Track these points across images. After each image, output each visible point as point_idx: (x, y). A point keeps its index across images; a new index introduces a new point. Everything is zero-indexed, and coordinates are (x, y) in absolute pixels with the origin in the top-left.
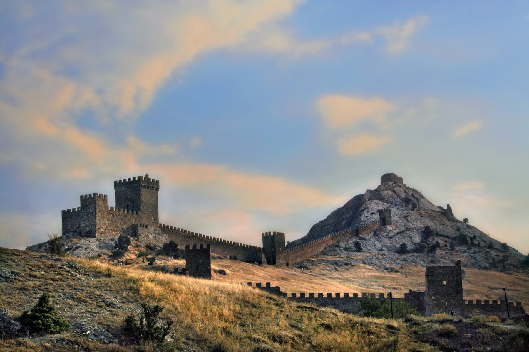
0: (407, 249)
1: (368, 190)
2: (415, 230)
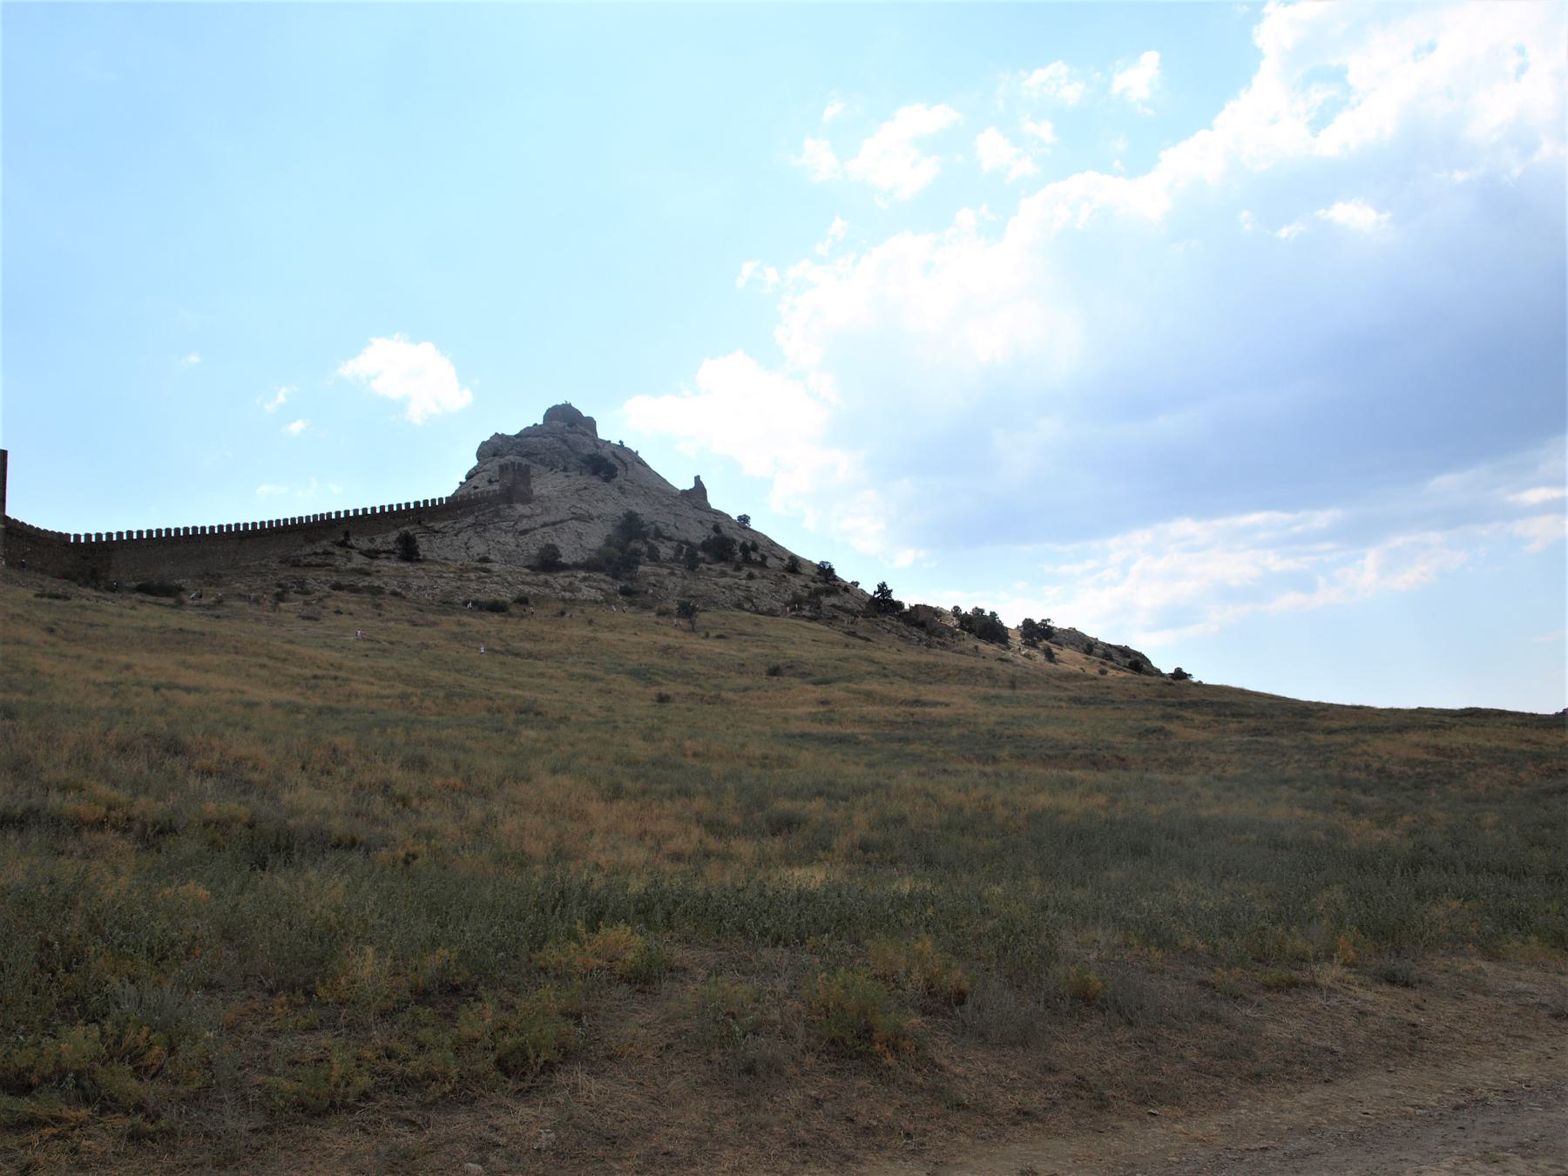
0: (560, 559)
1: (496, 434)
2: (596, 520)
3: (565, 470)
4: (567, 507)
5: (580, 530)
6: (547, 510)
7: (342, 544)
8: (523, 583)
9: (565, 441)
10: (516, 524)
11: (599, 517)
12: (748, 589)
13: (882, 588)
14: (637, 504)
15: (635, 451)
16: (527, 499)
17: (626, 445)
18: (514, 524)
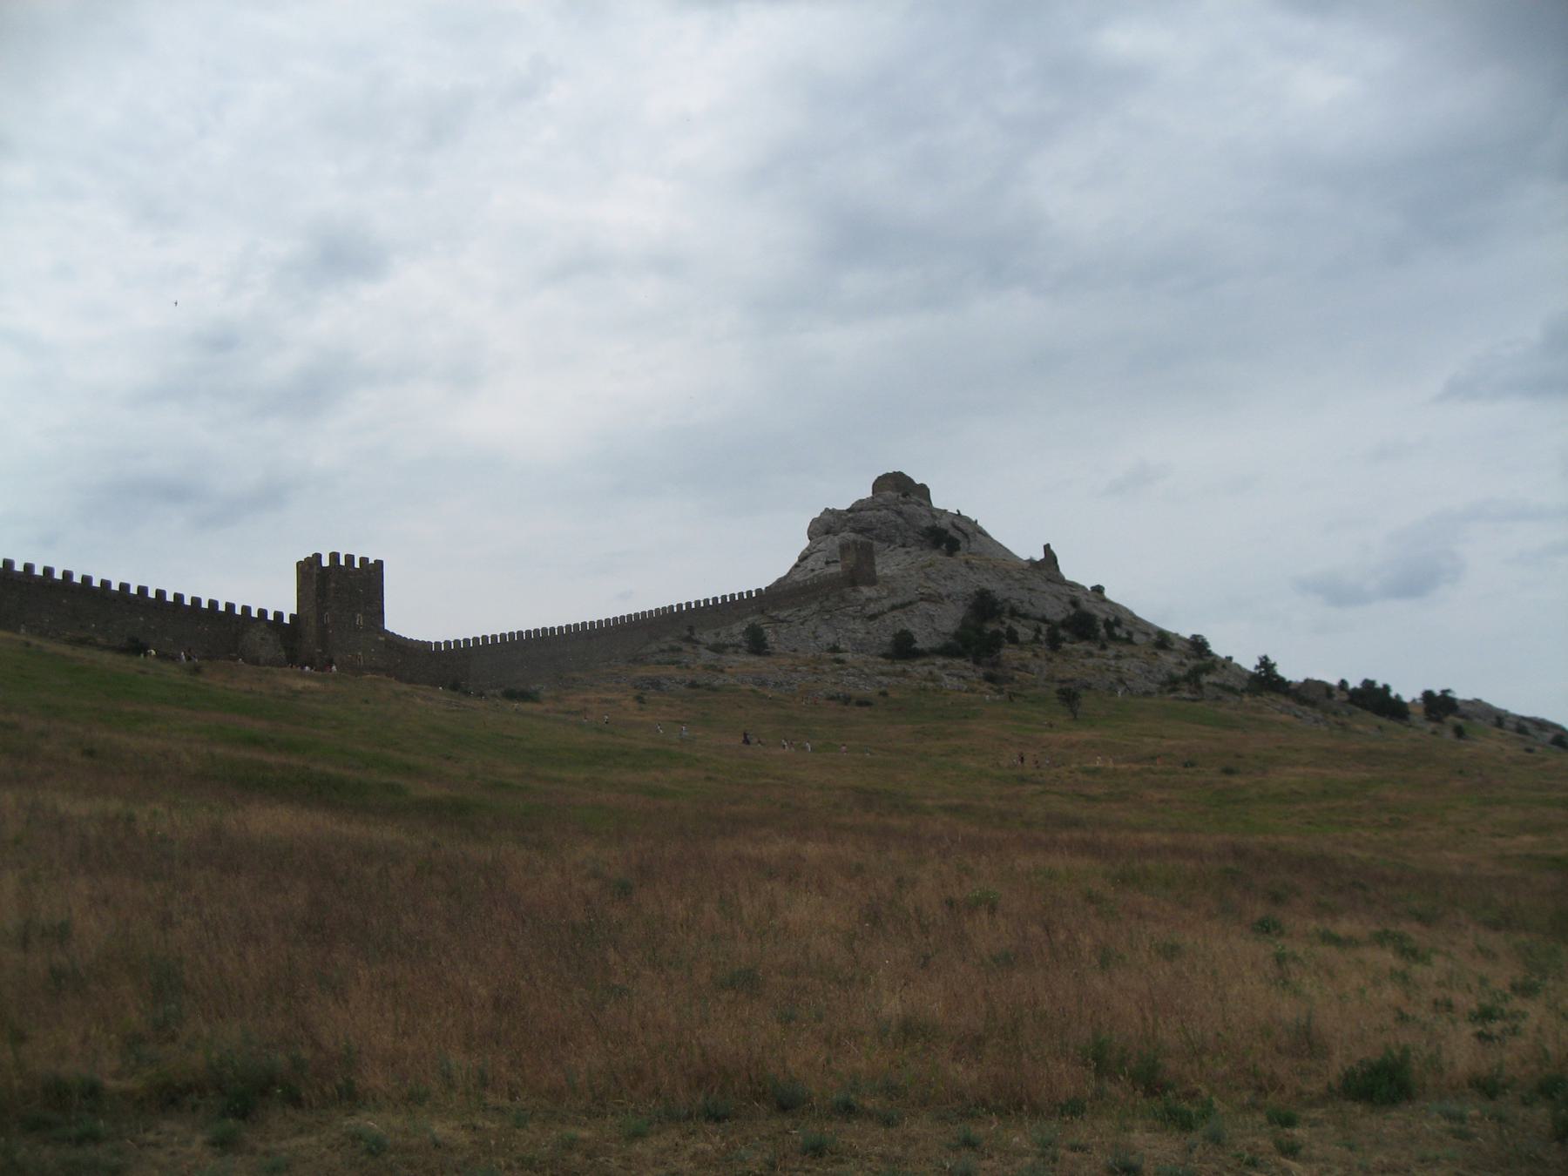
1: (827, 509)
2: (946, 599)
3: (904, 546)
4: (915, 586)
5: (931, 613)
6: (893, 592)
7: (688, 639)
8: (882, 674)
9: (900, 513)
10: (863, 608)
11: (948, 596)
12: (1118, 670)
13: (1265, 664)
14: (987, 580)
15: (974, 520)
16: (872, 581)
17: (963, 513)
18: (862, 609)
